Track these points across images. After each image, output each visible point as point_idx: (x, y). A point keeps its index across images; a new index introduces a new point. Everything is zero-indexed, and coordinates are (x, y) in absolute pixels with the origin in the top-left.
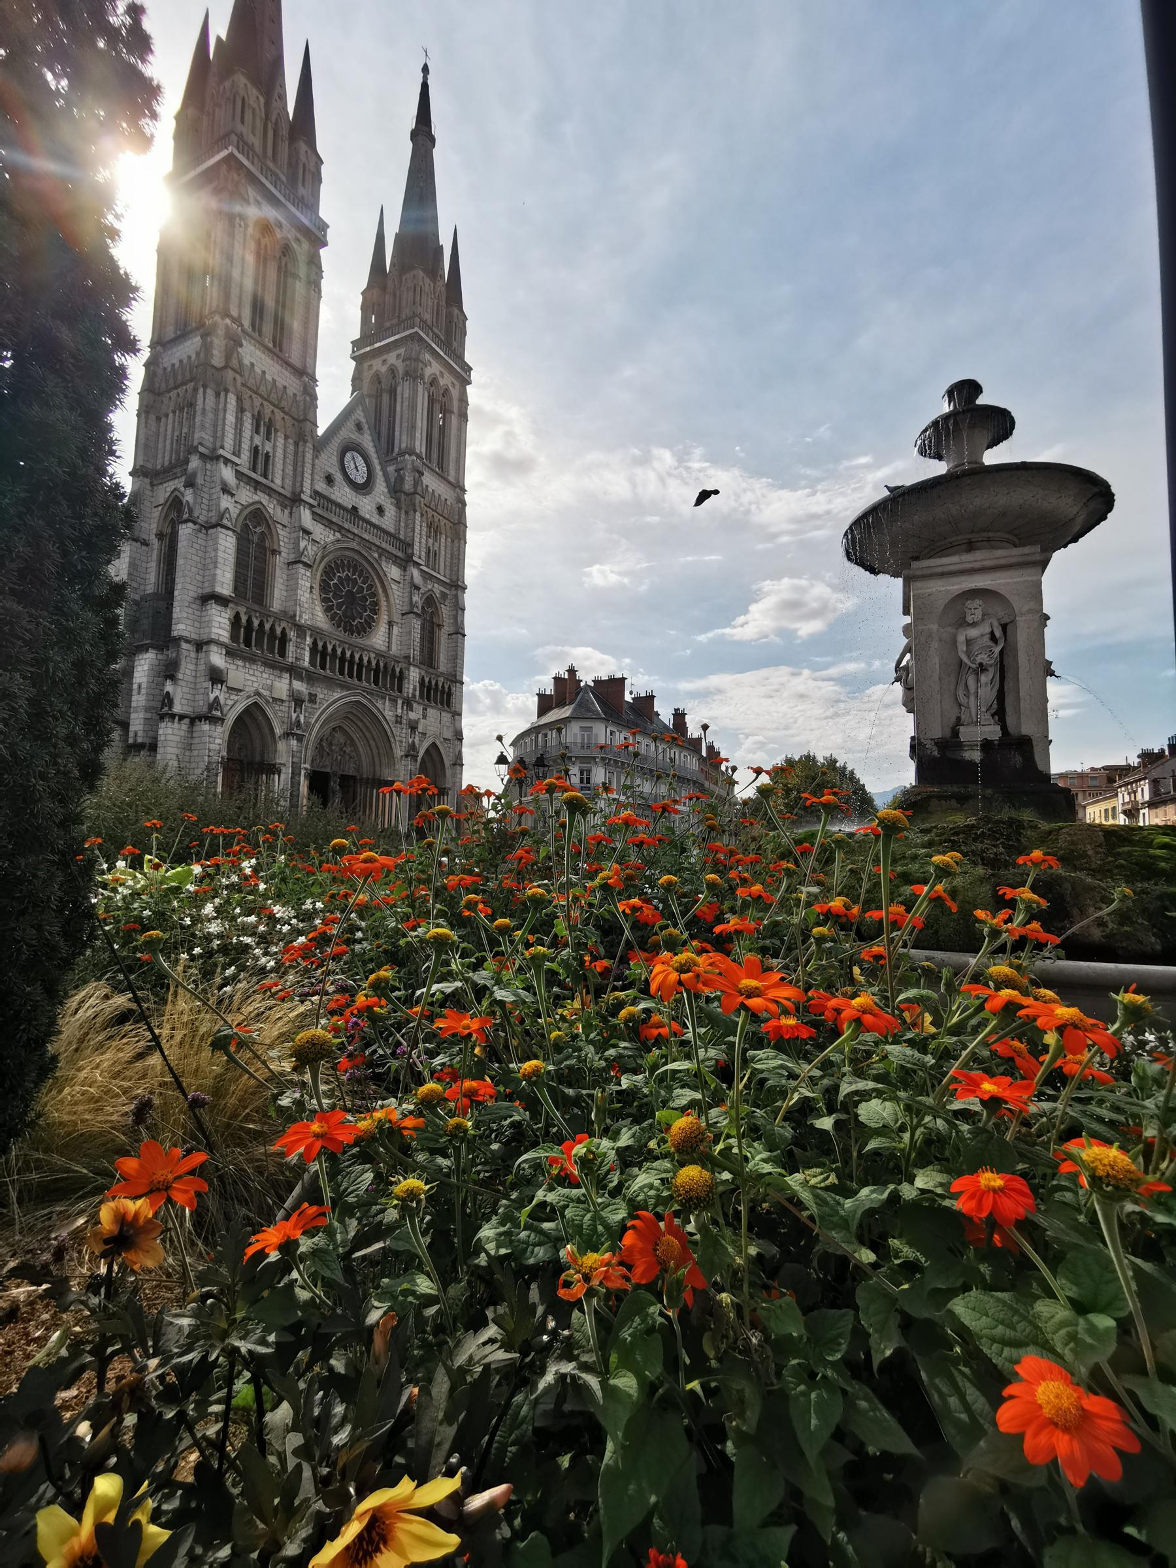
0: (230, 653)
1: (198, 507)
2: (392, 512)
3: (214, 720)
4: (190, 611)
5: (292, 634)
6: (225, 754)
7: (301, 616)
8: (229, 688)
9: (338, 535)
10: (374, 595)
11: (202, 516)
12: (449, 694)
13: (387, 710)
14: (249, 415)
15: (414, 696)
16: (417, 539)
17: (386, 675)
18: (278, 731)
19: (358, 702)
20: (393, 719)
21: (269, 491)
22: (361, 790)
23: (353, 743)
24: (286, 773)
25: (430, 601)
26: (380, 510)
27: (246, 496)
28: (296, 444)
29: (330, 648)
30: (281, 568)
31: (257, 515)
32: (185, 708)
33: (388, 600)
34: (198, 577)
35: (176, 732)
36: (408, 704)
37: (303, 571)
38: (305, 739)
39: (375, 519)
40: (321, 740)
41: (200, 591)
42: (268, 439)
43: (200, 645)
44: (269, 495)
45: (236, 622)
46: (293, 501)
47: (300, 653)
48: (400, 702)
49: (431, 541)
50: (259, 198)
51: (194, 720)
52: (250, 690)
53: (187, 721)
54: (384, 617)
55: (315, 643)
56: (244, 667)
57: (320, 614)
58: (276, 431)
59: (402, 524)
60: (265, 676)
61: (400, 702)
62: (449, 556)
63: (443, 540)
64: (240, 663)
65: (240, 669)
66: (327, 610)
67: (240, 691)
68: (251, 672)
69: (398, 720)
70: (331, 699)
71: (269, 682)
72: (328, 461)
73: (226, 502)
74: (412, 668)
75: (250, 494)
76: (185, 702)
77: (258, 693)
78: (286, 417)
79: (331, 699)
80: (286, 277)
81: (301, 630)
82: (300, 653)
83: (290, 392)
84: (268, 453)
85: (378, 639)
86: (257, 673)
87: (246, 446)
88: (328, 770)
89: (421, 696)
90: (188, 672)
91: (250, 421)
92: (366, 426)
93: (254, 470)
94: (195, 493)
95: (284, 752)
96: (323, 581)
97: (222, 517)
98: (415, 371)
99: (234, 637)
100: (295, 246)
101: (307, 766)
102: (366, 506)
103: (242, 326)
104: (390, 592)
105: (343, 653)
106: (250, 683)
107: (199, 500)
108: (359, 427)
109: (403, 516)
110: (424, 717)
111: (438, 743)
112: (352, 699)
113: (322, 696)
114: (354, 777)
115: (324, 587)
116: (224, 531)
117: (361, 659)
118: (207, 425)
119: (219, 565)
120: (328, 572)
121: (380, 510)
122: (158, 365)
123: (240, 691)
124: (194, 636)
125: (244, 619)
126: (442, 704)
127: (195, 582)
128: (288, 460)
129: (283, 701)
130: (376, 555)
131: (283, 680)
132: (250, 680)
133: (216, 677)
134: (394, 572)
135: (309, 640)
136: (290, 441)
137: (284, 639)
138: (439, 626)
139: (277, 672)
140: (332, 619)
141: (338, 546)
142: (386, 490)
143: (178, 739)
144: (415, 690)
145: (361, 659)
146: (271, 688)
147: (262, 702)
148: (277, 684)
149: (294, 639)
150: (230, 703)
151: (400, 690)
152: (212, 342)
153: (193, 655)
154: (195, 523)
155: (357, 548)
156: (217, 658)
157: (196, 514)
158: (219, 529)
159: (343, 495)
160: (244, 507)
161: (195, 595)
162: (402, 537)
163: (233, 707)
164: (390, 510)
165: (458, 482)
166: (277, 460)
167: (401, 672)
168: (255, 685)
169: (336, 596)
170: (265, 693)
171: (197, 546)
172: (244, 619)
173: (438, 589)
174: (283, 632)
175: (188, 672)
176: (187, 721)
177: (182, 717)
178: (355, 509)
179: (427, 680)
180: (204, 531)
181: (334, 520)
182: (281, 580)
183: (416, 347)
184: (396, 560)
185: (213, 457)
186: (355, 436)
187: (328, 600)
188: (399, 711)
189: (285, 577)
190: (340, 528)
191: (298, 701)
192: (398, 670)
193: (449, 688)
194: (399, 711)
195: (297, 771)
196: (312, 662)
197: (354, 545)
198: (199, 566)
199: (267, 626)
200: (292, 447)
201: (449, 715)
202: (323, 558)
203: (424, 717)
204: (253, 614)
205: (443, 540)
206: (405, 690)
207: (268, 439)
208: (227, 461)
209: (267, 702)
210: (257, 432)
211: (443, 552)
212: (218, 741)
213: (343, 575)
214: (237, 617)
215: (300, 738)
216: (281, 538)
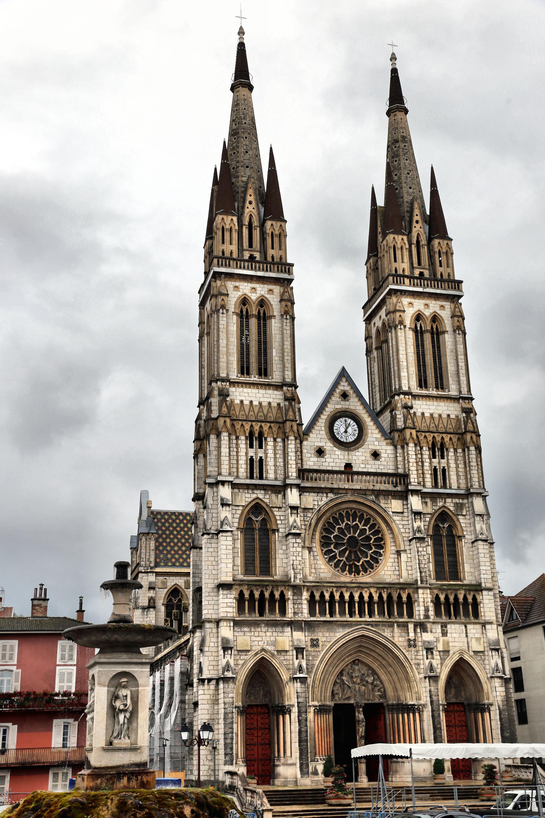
0: (237, 623)
1: (210, 521)
2: (389, 452)
3: (226, 680)
4: (210, 598)
5: (289, 594)
6: (240, 704)
7: (295, 577)
8: (239, 651)
9: (331, 495)
10: (378, 532)
11: (212, 526)
12: (476, 604)
13: (397, 638)
14: (243, 438)
15: (427, 616)
16: (413, 468)
17: (395, 602)
18: (285, 676)
19: (363, 636)
20: (406, 644)
21: (264, 488)
22: (389, 716)
23: (374, 673)
24: (295, 710)
25: (443, 516)
26: (376, 455)
27: (246, 498)
28: (284, 441)
29: (327, 596)
30: (280, 542)
31: (257, 508)
32: (212, 672)
33: (392, 533)
34: (214, 572)
35: (206, 692)
36: (422, 626)
37: (294, 540)
38: (310, 681)
39: (373, 466)
40: (341, 673)
41: (216, 581)
42: (261, 447)
43: (217, 622)
44: (264, 490)
45: (241, 599)
46: (281, 489)
47: (299, 608)
48: (411, 626)
49: (435, 461)
50: (237, 284)
51: (218, 680)
52: (257, 648)
53: (214, 682)
54: (390, 548)
55: (312, 596)
56: (251, 631)
57: (323, 567)
58: (266, 439)
59: (400, 459)
60: (268, 634)
61: (411, 626)
62: (461, 466)
63: (451, 454)
64: (246, 629)
65: (248, 634)
66: (331, 559)
67: (248, 651)
68: (256, 634)
69: (411, 644)
70: (331, 639)
71: (273, 639)
72: (318, 437)
73: (225, 513)
74: (420, 591)
75: (247, 495)
76: (211, 668)
77: (263, 650)
78: (272, 425)
79: (331, 639)
80: (265, 320)
81: (297, 589)
82: (299, 608)
83: (274, 404)
84: (261, 458)
85: (387, 571)
86: (261, 634)
87: (243, 461)
88: (352, 701)
89: (438, 613)
90: (212, 644)
91: (244, 442)
92: (351, 392)
93: (252, 477)
94: (207, 513)
95: (292, 694)
96: (323, 537)
97: (222, 523)
98: (394, 321)
99: (240, 609)
100: (268, 296)
101: (316, 703)
102: (360, 459)
103: (228, 381)
104: (393, 526)
105: (342, 596)
106: (256, 643)
107: (210, 516)
108: (345, 396)
109: (400, 451)
110: (444, 634)
111: (466, 657)
112: (356, 634)
113: (324, 639)
114: (381, 704)
115: (325, 542)
116: (224, 534)
117: (361, 596)
118: (212, 461)
119: (223, 561)
120: (328, 529)
121: (376, 455)
122: (201, 419)
123: (248, 651)
124: (214, 616)
125: (247, 595)
126: (466, 615)
127: (212, 577)
128: (278, 456)
129: (286, 651)
130: (372, 497)
131: (285, 634)
132: (259, 640)
133: (226, 647)
134: (396, 505)
135: (306, 595)
136: (279, 440)
137: (283, 600)
138: (459, 537)
139: (279, 629)
140: (336, 566)
141: (331, 504)
142: (379, 436)
143: (208, 697)
144: (427, 610)
145: (361, 596)
146: (274, 643)
147: (267, 657)
148: (280, 639)
149: (291, 598)
150: (241, 662)
151: (411, 614)
152: (211, 402)
153: (215, 630)
154: (208, 534)
155: (352, 498)
156: (226, 631)
157: (208, 528)
158: (221, 534)
159: (335, 459)
160: (245, 507)
161: (213, 586)
162: (401, 471)
163: (242, 667)
164: (386, 450)
165: (460, 392)
166: (269, 459)
167: (409, 597)
168: (260, 643)
169: (337, 546)
170: (269, 648)
171: (212, 550)
172: (247, 595)
173: (450, 504)
174: (282, 595)
175: (212, 644)
176: (214, 682)
177: (210, 680)
178: (348, 466)
179: (442, 597)
180: (215, 537)
181: (323, 486)
182: (281, 551)
183: (394, 299)
184: (396, 495)
185: (218, 483)
186: (343, 405)
187: (332, 551)
188: (412, 635)
189: (284, 547)
190: (332, 490)
191: (299, 650)
192: (404, 599)
193: (474, 599)
194: (412, 635)
195: (303, 709)
196: (312, 612)
197: (349, 497)
198: (214, 563)
199: (267, 595)
200: (281, 444)
201: (478, 627)
202: (318, 520)
203: (444, 634)
204: (254, 588)
205: (451, 454)
206: (416, 613)
207: (261, 447)
208: (223, 483)
209: (273, 655)
210: (251, 446)
211: (453, 465)
212: (230, 695)
213: (343, 526)
214: (241, 594)
215: (303, 680)
216: (278, 518)
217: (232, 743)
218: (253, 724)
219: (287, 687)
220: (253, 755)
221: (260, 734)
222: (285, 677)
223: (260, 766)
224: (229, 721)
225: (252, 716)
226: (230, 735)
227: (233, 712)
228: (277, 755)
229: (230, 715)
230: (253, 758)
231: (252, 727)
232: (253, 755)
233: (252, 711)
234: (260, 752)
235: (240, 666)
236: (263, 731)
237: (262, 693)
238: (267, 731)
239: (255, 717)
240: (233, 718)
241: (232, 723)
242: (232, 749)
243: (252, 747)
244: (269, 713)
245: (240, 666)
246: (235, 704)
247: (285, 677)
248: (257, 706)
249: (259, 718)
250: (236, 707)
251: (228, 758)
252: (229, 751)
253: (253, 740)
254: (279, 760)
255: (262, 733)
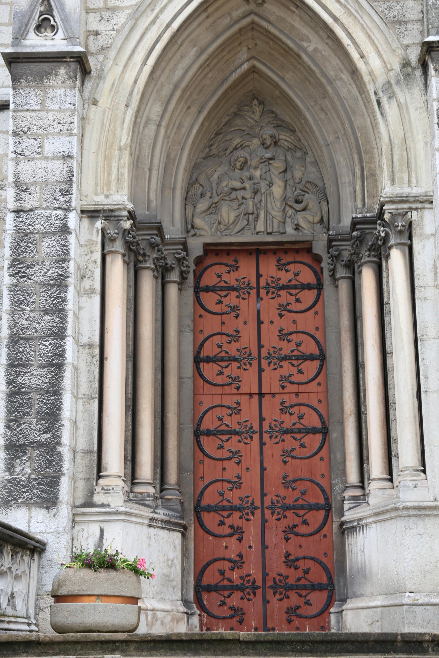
212: (52, 146)
217: (54, 391)
218: (235, 337)
219: (391, 109)
220: (237, 484)
221: (271, 383)
222: (375, 62)
223: (274, 537)
224: (40, 275)
225: (232, 299)
226: (45, 347)
227: (65, 230)
228: (353, 477)
229: (47, 246)
230: (234, 497)
231: (233, 349)
232: (237, 484)
233: (231, 279)
234: (275, 470)
235: (121, 18)
236: (287, 368)
237: (277, 190)
238: (311, 367)
239: (248, 306)
240: (63, 258)
241: (60, 282)
242: (52, 417)
243: (234, 444)
244: (320, 287)
245: (121, 18)
246: (91, 191)
247: (375, 62)
248: (257, 250)
249: (269, 307)
250: (91, 214)
251: (25, 469)
252: (32, 428)
253: (236, 410)
254: (361, 499)
255: (286, 380)
